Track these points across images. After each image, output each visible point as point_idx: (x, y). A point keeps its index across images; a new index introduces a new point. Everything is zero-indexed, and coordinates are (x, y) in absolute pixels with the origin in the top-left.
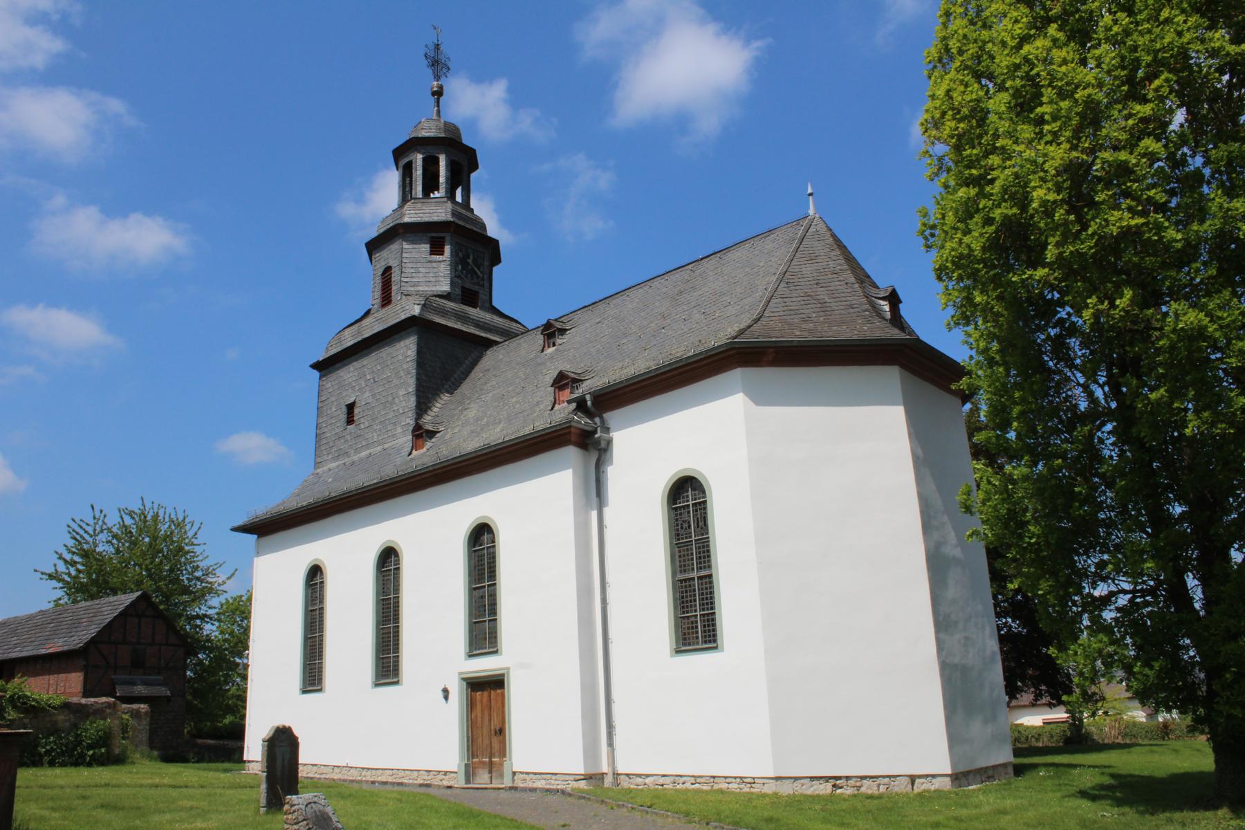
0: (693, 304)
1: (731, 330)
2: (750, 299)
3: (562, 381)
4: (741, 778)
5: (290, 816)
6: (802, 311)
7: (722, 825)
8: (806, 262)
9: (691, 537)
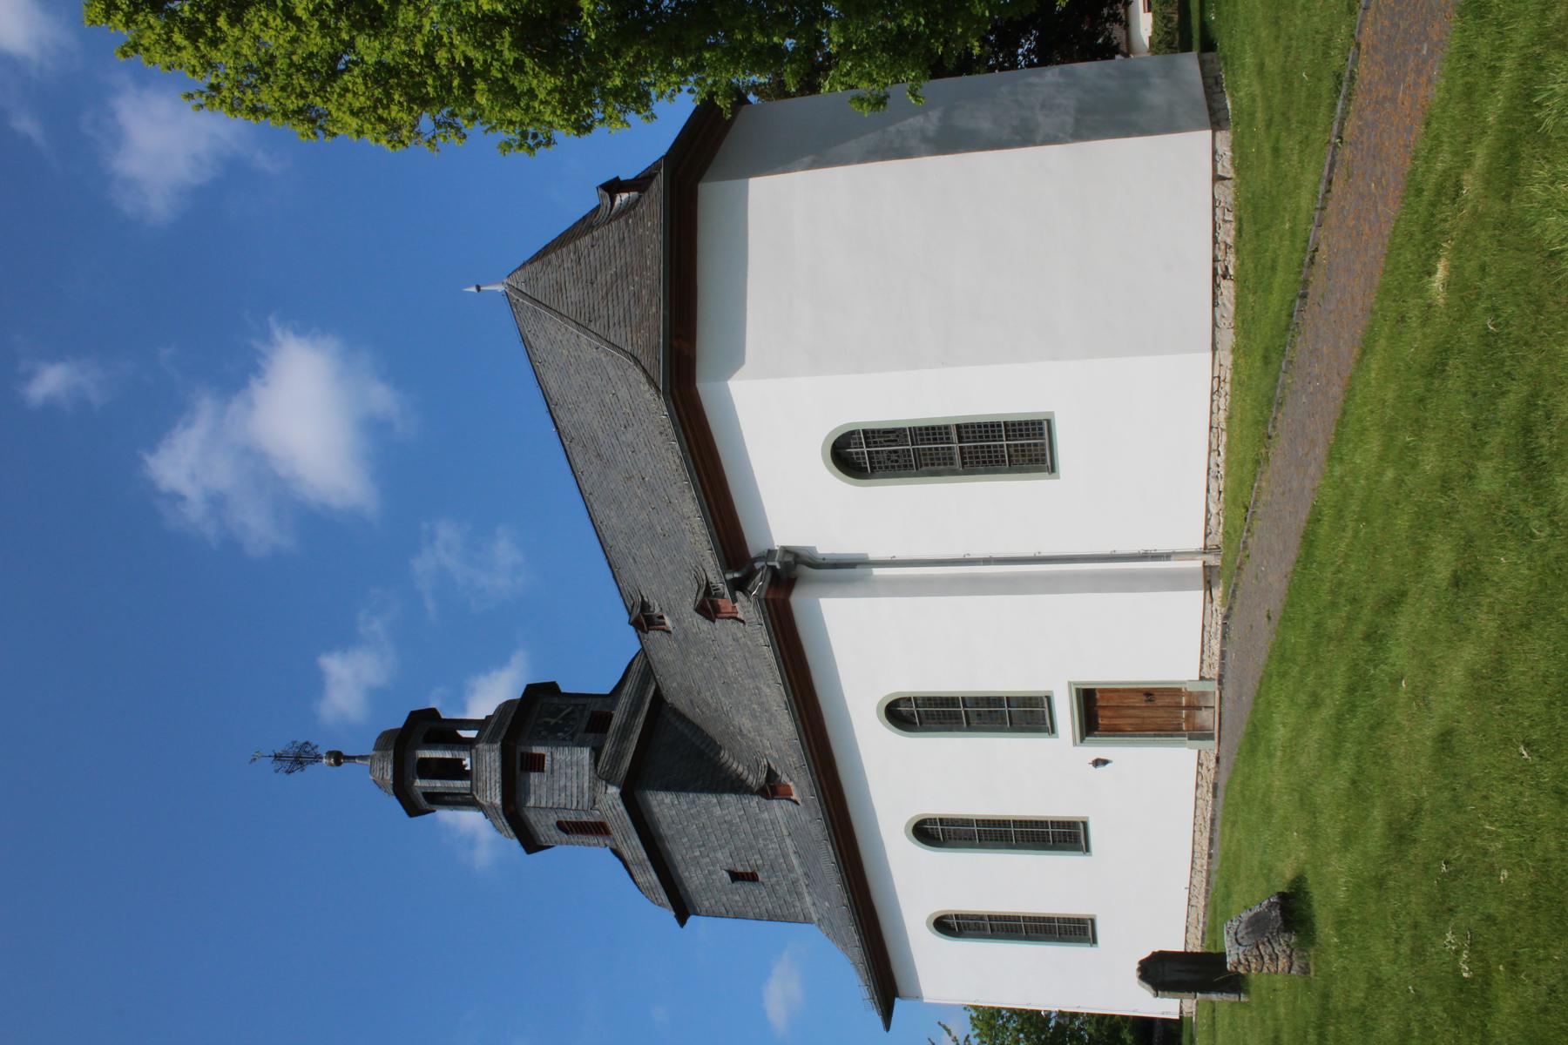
0: (614, 441)
1: (647, 393)
2: (609, 369)
3: (708, 608)
4: (1212, 394)
5: (1253, 966)
6: (626, 302)
7: (1271, 420)
8: (564, 296)
9: (908, 450)
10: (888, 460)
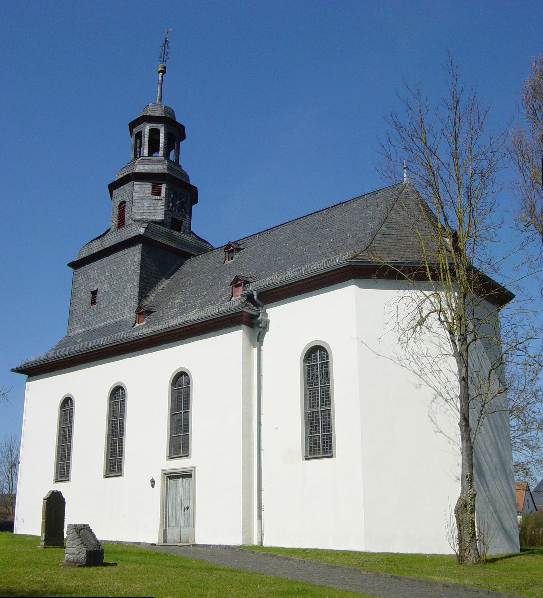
9: (318, 385)
10: (313, 374)
